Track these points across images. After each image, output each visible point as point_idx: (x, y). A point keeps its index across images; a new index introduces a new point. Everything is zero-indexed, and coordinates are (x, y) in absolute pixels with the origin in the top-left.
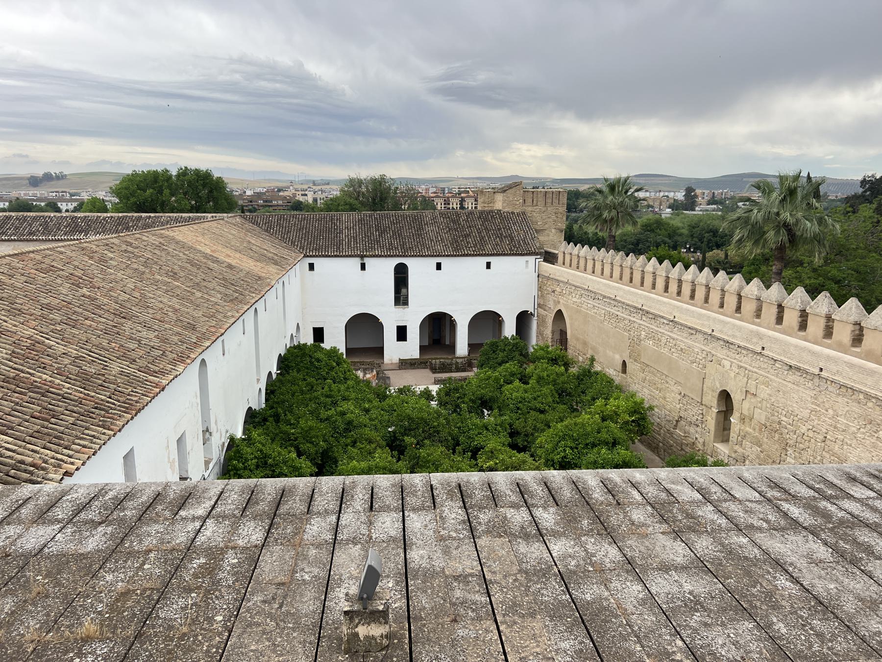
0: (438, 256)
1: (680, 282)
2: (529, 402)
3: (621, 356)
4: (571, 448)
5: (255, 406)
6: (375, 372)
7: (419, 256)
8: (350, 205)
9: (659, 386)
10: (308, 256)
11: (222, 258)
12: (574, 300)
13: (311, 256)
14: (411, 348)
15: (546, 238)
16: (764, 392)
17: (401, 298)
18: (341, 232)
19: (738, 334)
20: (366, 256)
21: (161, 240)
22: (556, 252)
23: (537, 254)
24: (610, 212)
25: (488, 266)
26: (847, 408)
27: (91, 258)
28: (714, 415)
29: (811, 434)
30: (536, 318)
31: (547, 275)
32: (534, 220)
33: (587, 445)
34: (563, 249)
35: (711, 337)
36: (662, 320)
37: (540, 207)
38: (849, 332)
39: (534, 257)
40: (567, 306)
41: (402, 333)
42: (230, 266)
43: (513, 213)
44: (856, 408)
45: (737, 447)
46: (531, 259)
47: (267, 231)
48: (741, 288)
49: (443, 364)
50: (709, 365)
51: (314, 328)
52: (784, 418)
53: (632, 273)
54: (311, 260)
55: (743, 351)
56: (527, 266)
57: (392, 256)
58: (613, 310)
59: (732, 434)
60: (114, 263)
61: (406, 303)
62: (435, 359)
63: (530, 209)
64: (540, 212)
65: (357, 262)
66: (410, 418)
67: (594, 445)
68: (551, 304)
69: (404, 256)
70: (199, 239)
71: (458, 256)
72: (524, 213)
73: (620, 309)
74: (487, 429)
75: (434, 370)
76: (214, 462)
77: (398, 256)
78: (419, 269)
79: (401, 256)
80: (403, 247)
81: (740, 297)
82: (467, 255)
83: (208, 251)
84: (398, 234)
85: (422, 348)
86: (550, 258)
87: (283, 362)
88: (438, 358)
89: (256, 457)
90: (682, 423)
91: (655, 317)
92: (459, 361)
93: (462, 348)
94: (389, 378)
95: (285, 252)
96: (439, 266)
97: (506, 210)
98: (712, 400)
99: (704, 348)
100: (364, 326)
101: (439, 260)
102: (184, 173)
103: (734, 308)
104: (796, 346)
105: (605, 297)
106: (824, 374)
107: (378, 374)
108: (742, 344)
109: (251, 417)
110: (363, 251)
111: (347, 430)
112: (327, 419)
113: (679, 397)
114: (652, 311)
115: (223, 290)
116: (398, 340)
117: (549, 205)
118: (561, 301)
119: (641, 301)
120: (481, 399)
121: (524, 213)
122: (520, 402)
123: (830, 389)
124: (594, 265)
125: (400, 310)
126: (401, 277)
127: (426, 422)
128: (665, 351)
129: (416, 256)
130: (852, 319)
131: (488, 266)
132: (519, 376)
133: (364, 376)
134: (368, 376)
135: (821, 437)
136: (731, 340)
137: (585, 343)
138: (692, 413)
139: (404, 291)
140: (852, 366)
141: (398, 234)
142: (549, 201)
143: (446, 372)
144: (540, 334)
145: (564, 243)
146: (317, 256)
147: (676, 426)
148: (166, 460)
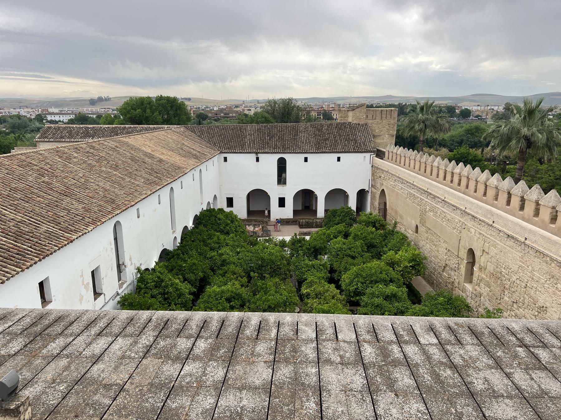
0: (305, 153)
1: (453, 173)
2: (345, 251)
3: (415, 221)
4: (362, 283)
5: (170, 248)
6: (261, 227)
7: (293, 153)
8: (265, 118)
9: (435, 243)
10: (223, 153)
11: (157, 155)
12: (391, 183)
13: (225, 153)
14: (288, 212)
15: (382, 141)
16: (493, 251)
17: (281, 179)
18: (245, 137)
19: (480, 212)
20: (259, 153)
21: (118, 145)
22: (384, 150)
23: (371, 152)
24: (419, 125)
25: (339, 159)
26: (540, 266)
27: (60, 157)
28: (465, 265)
29: (518, 282)
30: (370, 194)
31: (376, 166)
32: (373, 129)
33: (372, 281)
34: (391, 148)
35: (464, 213)
37: (378, 120)
38: (549, 213)
41: (282, 202)
42: (161, 161)
43: (359, 124)
44: (545, 267)
45: (477, 287)
46: (368, 155)
47: (199, 136)
48: (488, 179)
49: (307, 223)
50: (463, 231)
51: (227, 198)
52: (503, 270)
53: (426, 167)
54: (225, 155)
55: (482, 223)
57: (276, 153)
58: (412, 191)
59: (474, 278)
60: (75, 160)
61: (285, 183)
62: (303, 219)
63: (371, 121)
64: (378, 123)
65: (254, 156)
66: (263, 259)
67: (376, 282)
68: (378, 185)
69: (283, 153)
70: (148, 143)
71: (319, 153)
72: (366, 124)
73: (416, 191)
74: (314, 268)
75: (301, 226)
76: (128, 283)
77: (279, 153)
78: (294, 161)
79: (281, 153)
80: (283, 147)
81: (486, 186)
82: (324, 153)
83: (149, 151)
84: (281, 139)
85: (295, 212)
86: (380, 154)
87: (197, 220)
88: (304, 219)
89: (154, 281)
90: (448, 268)
91: (435, 197)
92: (318, 221)
93: (321, 213)
94: (269, 231)
95: (206, 150)
96: (306, 160)
97: (354, 122)
98: (464, 254)
99: (461, 219)
100: (258, 197)
101: (306, 155)
102: (160, 98)
103: (483, 193)
104: (512, 222)
105: (407, 182)
106: (527, 242)
107: (263, 228)
108: (481, 218)
109: (165, 255)
110: (257, 149)
111: (222, 265)
112: (211, 258)
113: (446, 251)
114: (433, 193)
115: (147, 176)
116: (279, 206)
117: (384, 118)
118: (384, 183)
119: (427, 186)
120: (314, 248)
121: (366, 124)
122: (339, 251)
123: (531, 252)
124: (405, 160)
125: (281, 187)
126: (282, 166)
127: (273, 262)
128: (439, 220)
129: (291, 153)
130: (551, 204)
131: (339, 159)
132: (343, 233)
133: (254, 229)
134: (257, 229)
135: (524, 285)
136: (476, 215)
137: (396, 212)
138: (453, 262)
139: (283, 175)
140: (544, 237)
141: (281, 139)
142: (384, 116)
143: (309, 228)
144: (372, 204)
145: (393, 146)
146: (228, 153)
147: (444, 270)
148: (81, 283)
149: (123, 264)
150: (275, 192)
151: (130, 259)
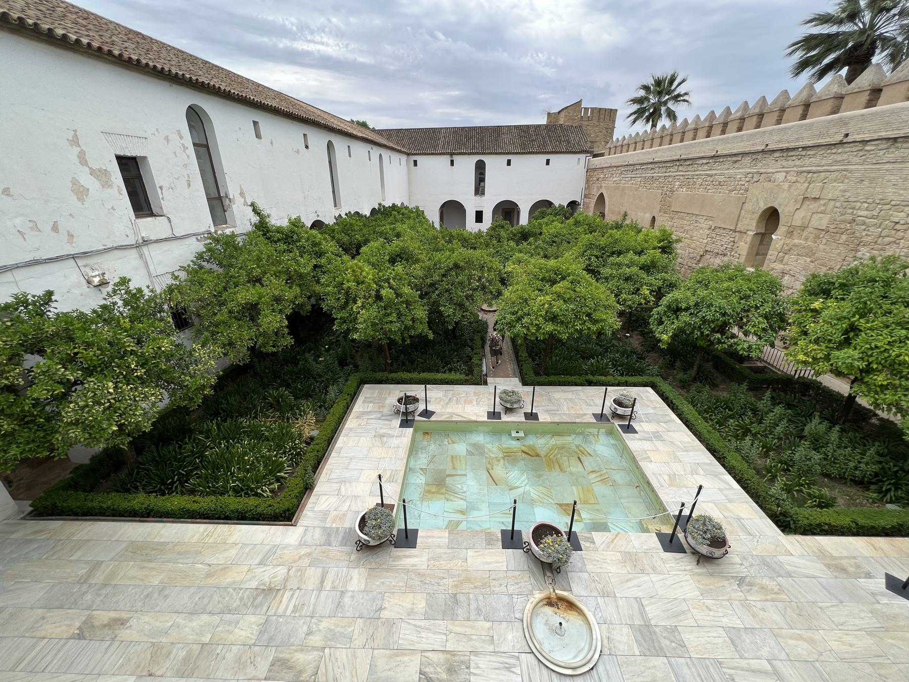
4: (597, 257)
17: (479, 190)
18: (439, 139)
25: (548, 162)
28: (749, 239)
36: (701, 162)
39: (584, 155)
40: (607, 188)
41: (479, 217)
46: (582, 157)
54: (415, 158)
56: (578, 163)
59: (770, 252)
61: (483, 194)
63: (586, 123)
65: (446, 159)
78: (494, 164)
87: (373, 211)
113: (708, 232)
116: (477, 221)
121: (580, 127)
122: (556, 236)
125: (478, 198)
142: (602, 117)
149: (227, 197)
150: (471, 204)
151: (242, 194)
